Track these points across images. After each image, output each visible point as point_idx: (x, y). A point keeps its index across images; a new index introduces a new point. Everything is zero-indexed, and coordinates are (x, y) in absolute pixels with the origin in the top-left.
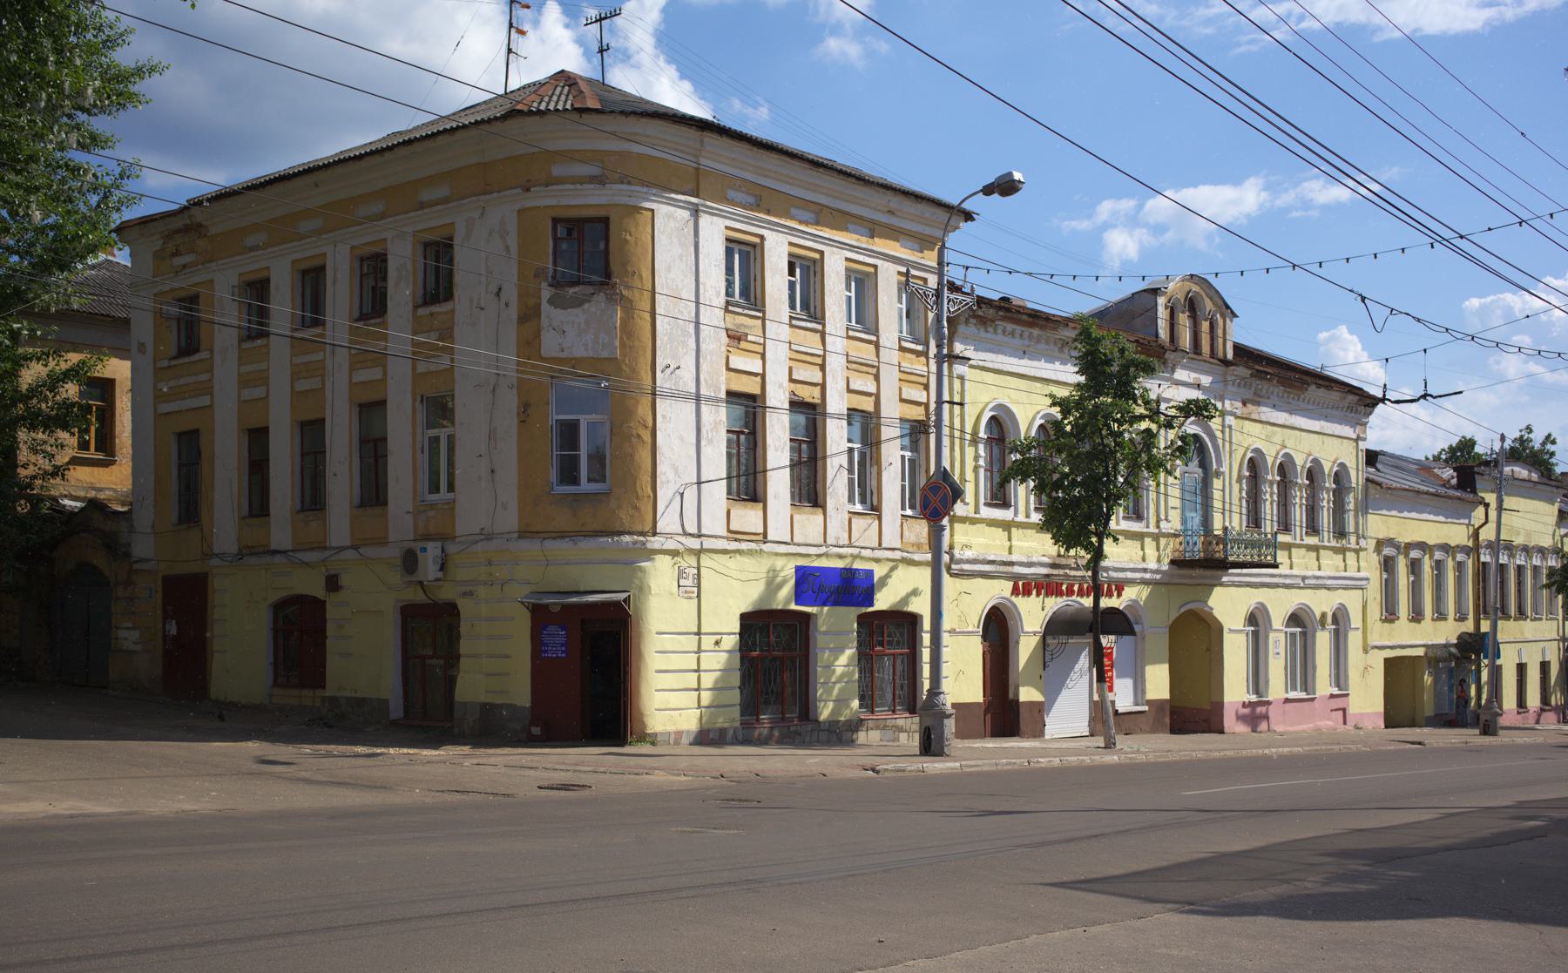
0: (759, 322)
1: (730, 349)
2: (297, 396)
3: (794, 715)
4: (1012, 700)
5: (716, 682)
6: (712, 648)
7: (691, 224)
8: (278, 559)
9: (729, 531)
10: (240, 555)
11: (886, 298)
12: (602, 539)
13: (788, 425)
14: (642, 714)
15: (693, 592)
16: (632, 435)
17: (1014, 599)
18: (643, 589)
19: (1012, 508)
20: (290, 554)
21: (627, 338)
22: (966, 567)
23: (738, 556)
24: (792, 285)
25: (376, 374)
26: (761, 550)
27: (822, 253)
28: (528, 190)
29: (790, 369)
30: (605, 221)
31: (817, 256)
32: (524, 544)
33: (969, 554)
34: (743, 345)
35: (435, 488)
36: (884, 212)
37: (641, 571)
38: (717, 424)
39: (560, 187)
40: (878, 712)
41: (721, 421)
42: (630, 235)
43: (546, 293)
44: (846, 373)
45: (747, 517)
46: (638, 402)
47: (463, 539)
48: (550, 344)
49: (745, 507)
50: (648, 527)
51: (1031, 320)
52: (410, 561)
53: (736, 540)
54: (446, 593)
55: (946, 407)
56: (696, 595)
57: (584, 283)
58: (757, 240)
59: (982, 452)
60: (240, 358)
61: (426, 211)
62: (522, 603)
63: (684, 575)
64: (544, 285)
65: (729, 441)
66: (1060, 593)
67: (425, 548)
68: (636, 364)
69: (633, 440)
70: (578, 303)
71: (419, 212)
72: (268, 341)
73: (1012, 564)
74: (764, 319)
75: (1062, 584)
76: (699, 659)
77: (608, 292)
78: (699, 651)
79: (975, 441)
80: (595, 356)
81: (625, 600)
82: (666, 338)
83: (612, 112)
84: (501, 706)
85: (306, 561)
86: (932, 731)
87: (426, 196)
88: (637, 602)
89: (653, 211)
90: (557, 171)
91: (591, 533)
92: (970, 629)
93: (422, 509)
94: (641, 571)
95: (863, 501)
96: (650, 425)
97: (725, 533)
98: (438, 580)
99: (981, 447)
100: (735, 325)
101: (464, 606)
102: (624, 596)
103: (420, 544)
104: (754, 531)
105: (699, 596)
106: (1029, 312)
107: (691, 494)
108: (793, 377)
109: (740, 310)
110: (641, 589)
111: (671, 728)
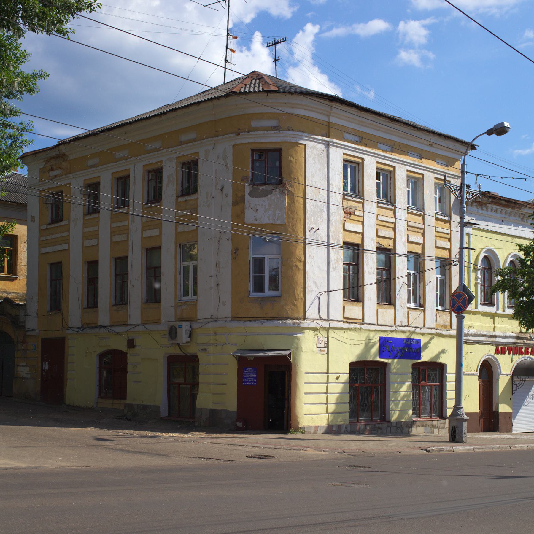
0: (361, 205)
1: (345, 219)
2: (114, 244)
3: (378, 418)
4: (495, 412)
5: (338, 398)
6: (335, 381)
7: (325, 152)
8: (102, 330)
9: (344, 318)
10: (83, 328)
11: (428, 192)
13: (375, 261)
14: (297, 416)
15: (325, 351)
16: (293, 266)
17: (496, 356)
18: (298, 349)
19: (496, 306)
20: (109, 328)
21: (291, 214)
22: (471, 338)
23: (348, 331)
24: (378, 185)
25: (155, 232)
26: (361, 328)
27: (394, 167)
28: (239, 134)
29: (377, 230)
30: (279, 151)
31: (392, 169)
32: (235, 324)
33: (472, 331)
34: (352, 217)
35: (186, 293)
36: (428, 145)
37: (297, 339)
38: (338, 260)
39: (256, 133)
40: (422, 417)
41: (340, 258)
42: (293, 158)
43: (248, 189)
44: (407, 232)
45: (354, 311)
46: (296, 248)
47: (202, 321)
48: (249, 216)
49: (353, 305)
50: (301, 315)
51: (506, 203)
52: (173, 332)
53: (348, 322)
54: (192, 350)
55: (465, 251)
56: (326, 352)
57: (268, 184)
58: (360, 161)
59: (479, 275)
60: (84, 224)
61: (184, 146)
62: (233, 355)
63: (320, 341)
65: (344, 269)
66: (521, 353)
67: (181, 326)
68: (296, 228)
69: (294, 268)
70: (265, 194)
71: (180, 147)
72: (99, 215)
73: (495, 337)
75: (522, 348)
76: (327, 387)
77: (280, 188)
78: (327, 383)
79: (475, 270)
80: (273, 223)
81: (289, 355)
82: (311, 213)
83: (284, 92)
84: (221, 411)
85: (117, 331)
86: (456, 429)
87: (184, 138)
88: (295, 356)
89: (305, 145)
90: (254, 124)
92: (473, 372)
93: (179, 304)
95: (415, 302)
96: (303, 260)
97: (341, 319)
98: (187, 342)
99: (479, 272)
101: (200, 356)
102: (288, 352)
103: (178, 324)
104: (357, 318)
105: (328, 353)
106: (506, 199)
107: (324, 298)
108: (379, 234)
110: (297, 348)
111: (312, 424)
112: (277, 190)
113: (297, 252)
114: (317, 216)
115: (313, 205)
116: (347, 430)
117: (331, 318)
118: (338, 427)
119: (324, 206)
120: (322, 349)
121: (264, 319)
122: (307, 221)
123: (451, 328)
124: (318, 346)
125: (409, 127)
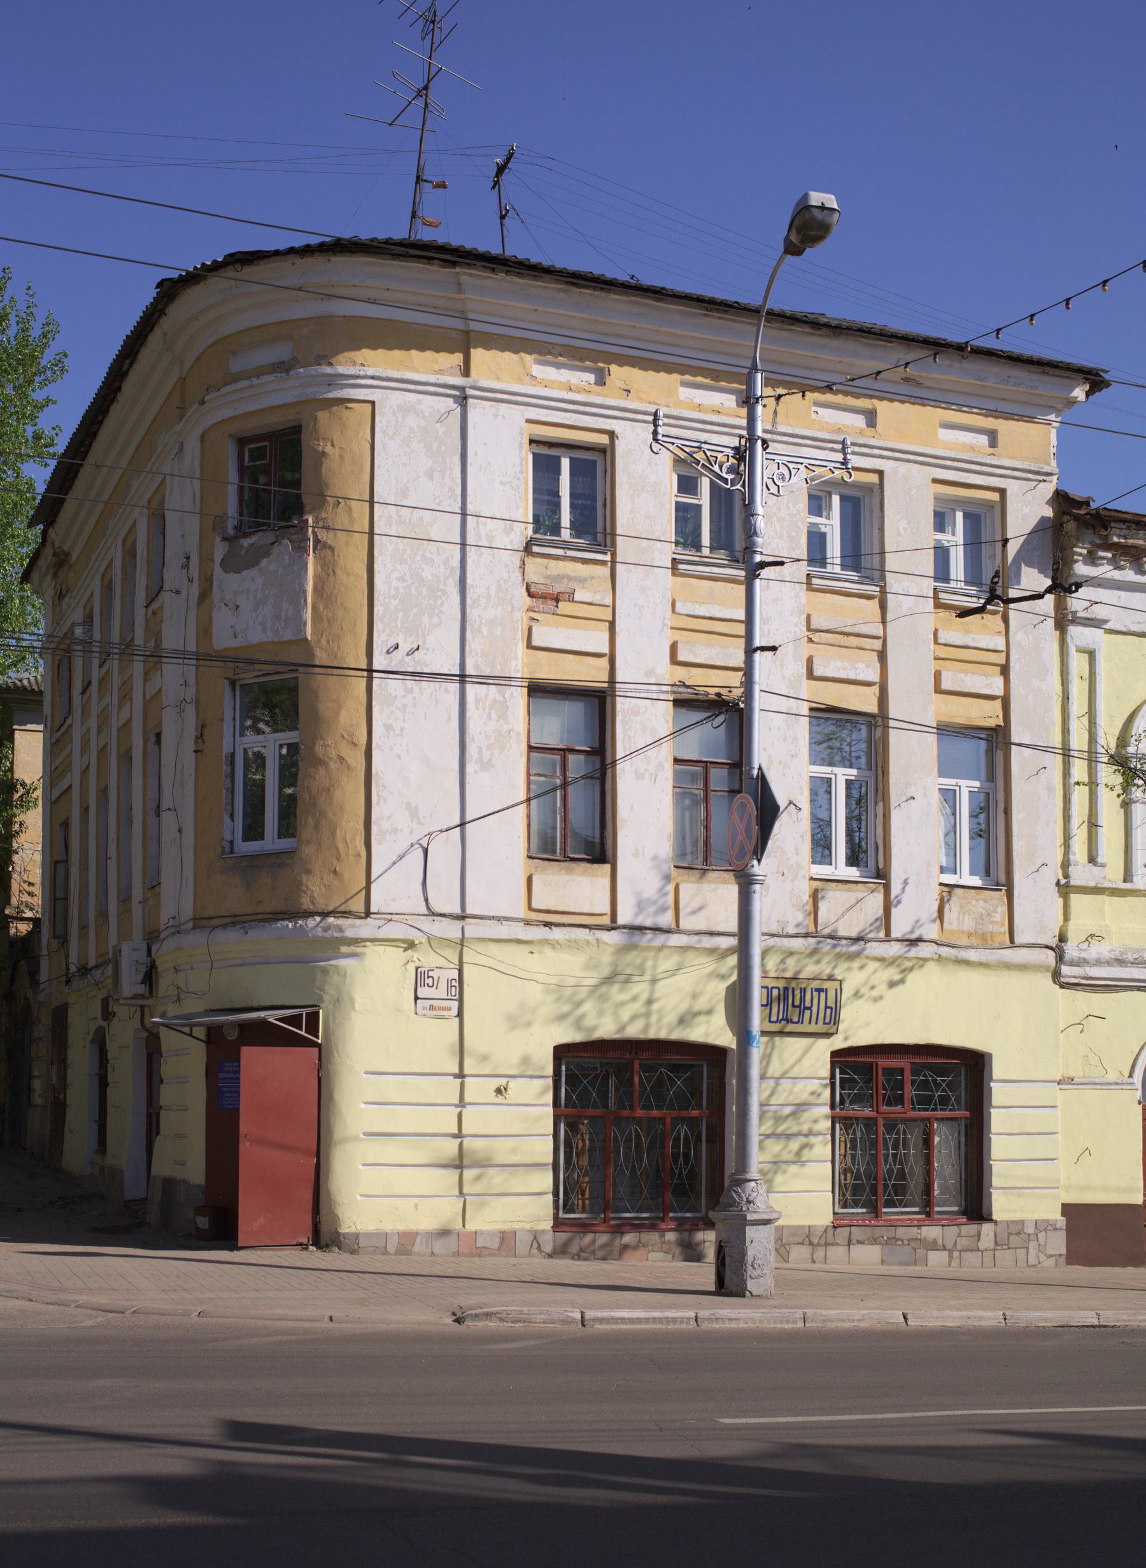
9: (530, 908)
11: (903, 524)
12: (280, 924)
14: (335, 1202)
15: (450, 1009)
16: (331, 759)
21: (326, 607)
23: (548, 951)
33: (1096, 950)
34: (564, 607)
36: (896, 382)
37: (339, 974)
41: (509, 731)
42: (333, 445)
43: (220, 550)
44: (807, 650)
46: (340, 707)
49: (569, 871)
50: (358, 905)
53: (547, 924)
56: (455, 1012)
58: (604, 439)
63: (430, 981)
64: (218, 539)
68: (339, 647)
69: (332, 765)
70: (253, 559)
74: (614, 562)
76: (460, 1116)
77: (294, 537)
78: (462, 1103)
80: (275, 640)
82: (395, 602)
88: (330, 1023)
89: (373, 403)
90: (237, 365)
91: (269, 916)
92: (1112, 1077)
94: (339, 974)
95: (853, 860)
96: (363, 740)
97: (521, 911)
100: (547, 577)
105: (460, 1014)
107: (445, 851)
109: (560, 552)
110: (338, 1001)
112: (286, 541)
113: (343, 717)
114: (415, 610)
115: (401, 579)
116: (539, 1248)
117: (469, 910)
119: (446, 578)
120: (436, 1003)
121: (255, 917)
122: (378, 626)
123: (1012, 940)
124: (419, 995)
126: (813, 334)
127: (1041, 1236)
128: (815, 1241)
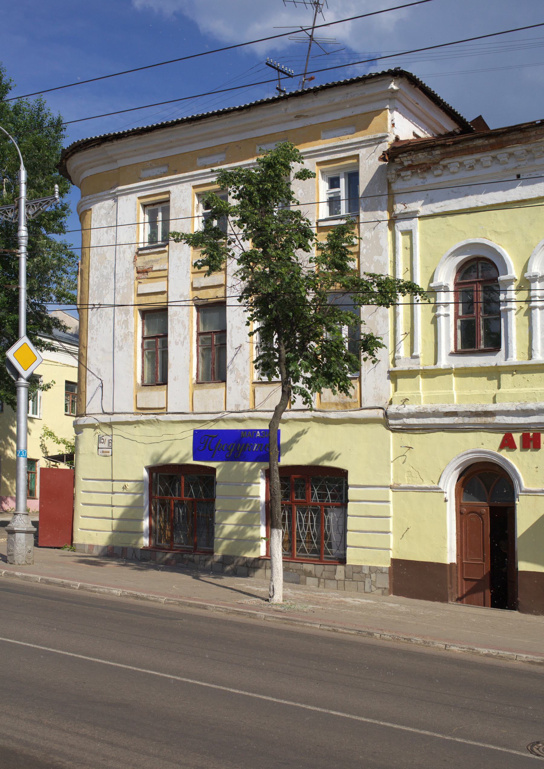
5: (124, 514)
6: (121, 490)
15: (109, 452)
23: (141, 426)
26: (157, 419)
34: (151, 275)
49: (151, 390)
63: (102, 441)
73: (492, 414)
82: (95, 287)
111: (88, 542)
115: (97, 277)
118: (123, 551)
119: (111, 273)
120: (104, 450)
125: (231, 115)
126: (240, 115)
127: (373, 575)
128: (249, 565)
